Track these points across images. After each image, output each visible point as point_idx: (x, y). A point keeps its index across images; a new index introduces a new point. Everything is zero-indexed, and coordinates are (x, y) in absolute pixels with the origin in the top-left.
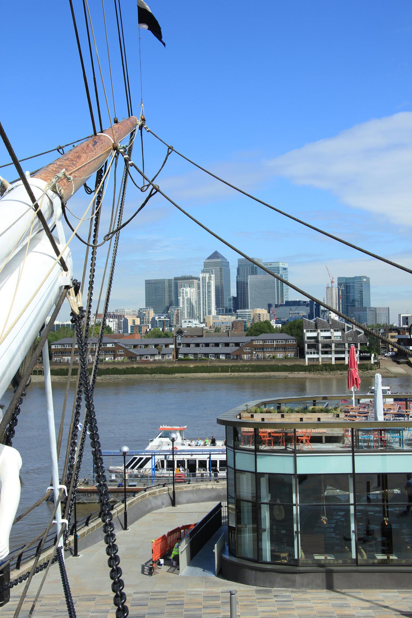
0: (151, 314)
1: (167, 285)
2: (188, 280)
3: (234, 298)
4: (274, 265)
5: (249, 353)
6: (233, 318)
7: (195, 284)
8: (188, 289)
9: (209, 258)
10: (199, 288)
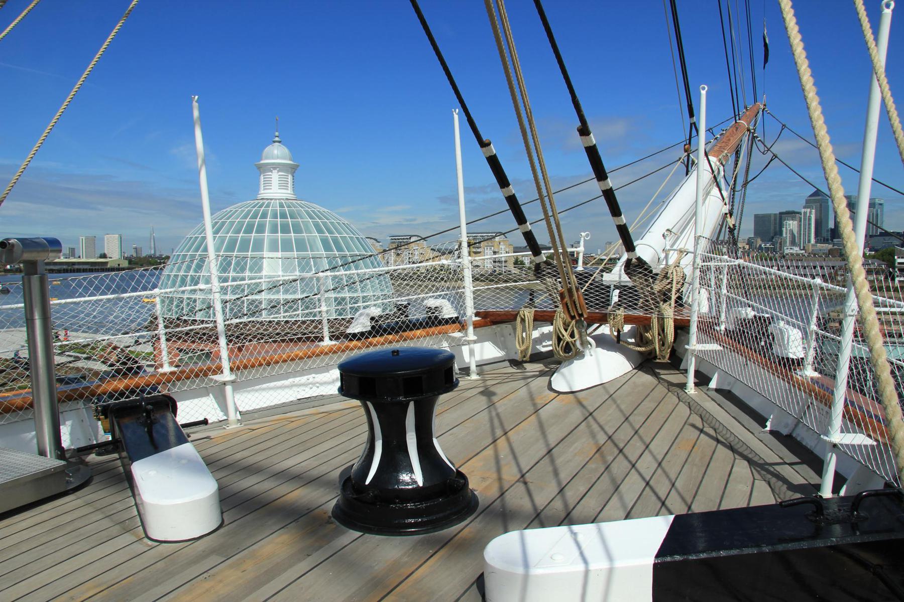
0: (759, 242)
1: (772, 218)
2: (792, 214)
3: (832, 230)
5: (842, 275)
6: (830, 246)
8: (791, 222)
9: (811, 196)
10: (800, 221)
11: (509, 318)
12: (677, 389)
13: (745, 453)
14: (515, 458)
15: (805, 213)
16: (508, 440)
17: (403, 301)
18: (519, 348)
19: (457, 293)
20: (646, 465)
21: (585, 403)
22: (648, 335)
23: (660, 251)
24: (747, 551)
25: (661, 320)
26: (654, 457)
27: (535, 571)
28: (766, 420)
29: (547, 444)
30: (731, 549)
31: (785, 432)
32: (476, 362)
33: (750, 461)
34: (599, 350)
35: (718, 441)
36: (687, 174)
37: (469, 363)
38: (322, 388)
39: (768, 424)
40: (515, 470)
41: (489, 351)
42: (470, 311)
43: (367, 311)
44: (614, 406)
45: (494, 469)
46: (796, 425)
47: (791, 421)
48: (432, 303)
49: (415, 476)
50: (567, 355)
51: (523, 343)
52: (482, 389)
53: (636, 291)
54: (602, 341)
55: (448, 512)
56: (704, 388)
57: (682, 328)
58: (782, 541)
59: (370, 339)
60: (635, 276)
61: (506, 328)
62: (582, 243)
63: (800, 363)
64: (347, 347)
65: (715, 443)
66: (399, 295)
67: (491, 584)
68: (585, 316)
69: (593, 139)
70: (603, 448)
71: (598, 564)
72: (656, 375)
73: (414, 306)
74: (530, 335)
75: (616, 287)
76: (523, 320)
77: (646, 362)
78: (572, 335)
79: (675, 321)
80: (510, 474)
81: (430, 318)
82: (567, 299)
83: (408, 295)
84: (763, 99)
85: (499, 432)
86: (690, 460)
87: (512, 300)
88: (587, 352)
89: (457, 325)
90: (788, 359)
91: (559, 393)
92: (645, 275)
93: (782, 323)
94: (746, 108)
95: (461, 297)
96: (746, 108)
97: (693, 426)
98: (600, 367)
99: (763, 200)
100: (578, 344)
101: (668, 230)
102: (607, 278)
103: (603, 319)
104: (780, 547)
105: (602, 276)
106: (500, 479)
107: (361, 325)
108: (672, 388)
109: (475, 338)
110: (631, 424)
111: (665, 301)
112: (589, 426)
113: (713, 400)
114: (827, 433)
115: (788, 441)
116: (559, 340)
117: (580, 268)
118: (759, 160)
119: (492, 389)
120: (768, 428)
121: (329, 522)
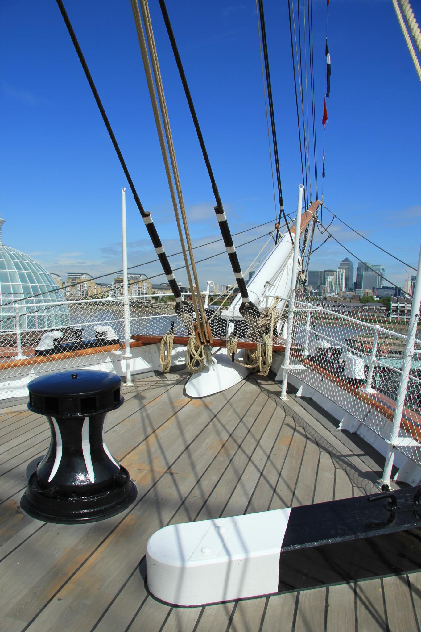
1: (320, 274)
2: (331, 272)
4: (377, 267)
6: (354, 293)
7: (335, 275)
8: (331, 277)
10: (336, 277)
11: (155, 341)
12: (274, 396)
13: (327, 447)
14: (163, 452)
15: (339, 272)
16: (156, 437)
19: (119, 322)
20: (259, 457)
21: (211, 407)
22: (253, 356)
23: (260, 296)
24: (347, 538)
25: (264, 346)
27: (189, 564)
28: (339, 422)
29: (185, 441)
30: (336, 537)
31: (352, 431)
32: (131, 372)
33: (330, 453)
34: (219, 365)
36: (276, 244)
37: (126, 373)
38: (15, 392)
39: (340, 425)
40: (163, 463)
41: (140, 364)
42: (128, 336)
43: (51, 334)
44: (232, 410)
46: (360, 426)
47: (356, 423)
48: (100, 328)
49: (88, 476)
50: (196, 368)
51: (165, 359)
52: (134, 394)
53: (247, 325)
54: (222, 360)
55: (113, 503)
57: (279, 351)
58: (369, 527)
59: (53, 355)
60: (247, 315)
61: (153, 347)
62: (208, 289)
63: (362, 383)
65: (305, 439)
66: (76, 323)
67: (151, 571)
68: (211, 342)
69: (225, 216)
70: (227, 444)
71: (238, 556)
72: (259, 385)
73: (87, 331)
74: (169, 353)
75: (231, 321)
76: (166, 343)
77: (251, 375)
78: (201, 355)
79: (274, 347)
80: (160, 466)
81: (98, 340)
82: (199, 330)
83: (83, 322)
84: (322, 198)
85: (149, 430)
86: (289, 453)
87: (158, 328)
88: (211, 368)
89: (118, 345)
90: (356, 380)
91: (192, 398)
92: (254, 314)
93: (350, 355)
94: (311, 202)
95: (121, 325)
97: (288, 425)
98: (219, 379)
99: (317, 264)
100: (205, 361)
101: (267, 282)
102: (226, 314)
103: (222, 344)
104: (371, 534)
105: (221, 312)
106: (152, 471)
107: (46, 344)
108: (271, 395)
110: (245, 425)
111: (267, 333)
112: (214, 426)
113: (300, 405)
114: (389, 438)
115: (354, 437)
116: (191, 358)
117: (206, 306)
119: (143, 394)
120: (340, 428)
121: (18, 513)
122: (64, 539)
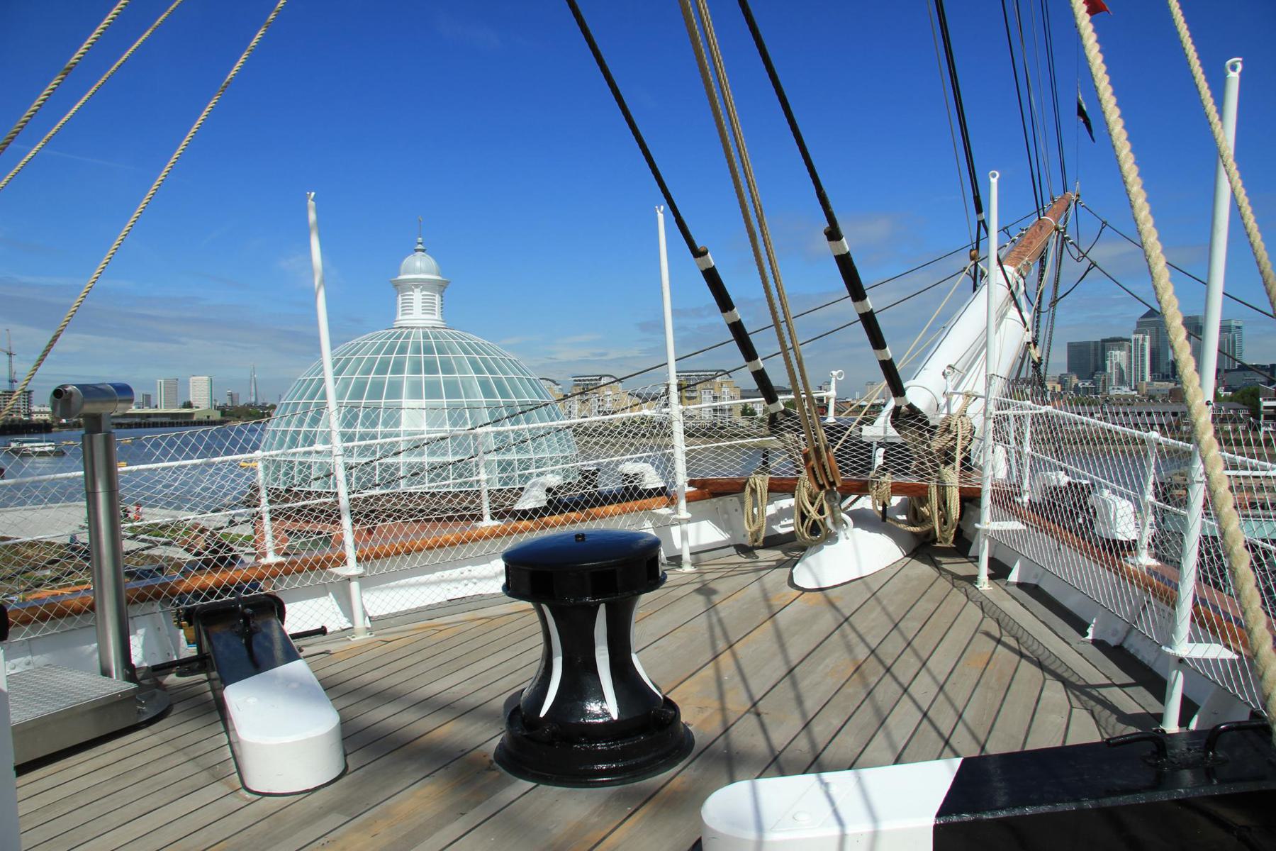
0: (1075, 380)
1: (1092, 347)
2: (1118, 342)
8: (1118, 353)
9: (1144, 317)
11: (733, 488)
12: (964, 584)
13: (1059, 671)
16: (734, 655)
17: (590, 465)
18: (748, 529)
19: (664, 455)
20: (923, 689)
21: (839, 604)
22: (924, 509)
23: (939, 395)
24: (1061, 807)
25: (942, 489)
26: (934, 678)
28: (1087, 626)
29: (787, 661)
31: (1113, 641)
33: (1067, 684)
34: (858, 530)
35: (1022, 655)
37: (681, 550)
38: (480, 584)
39: (1090, 631)
41: (708, 533)
42: (682, 479)
43: (542, 479)
44: (879, 609)
45: (715, 695)
47: (1121, 628)
48: (629, 468)
49: (607, 706)
52: (698, 586)
54: (861, 519)
55: (651, 755)
56: (1001, 582)
57: (970, 499)
59: (546, 518)
61: (731, 501)
62: (833, 385)
63: (1131, 546)
64: (515, 529)
65: (1017, 658)
66: (586, 458)
68: (838, 485)
69: (846, 245)
70: (864, 666)
71: (858, 827)
72: (936, 565)
74: (763, 512)
75: (880, 445)
76: (754, 491)
77: (922, 548)
78: (821, 511)
79: (961, 490)
80: (737, 702)
81: (627, 489)
82: (813, 462)
83: (598, 457)
85: (721, 645)
86: (982, 681)
87: (738, 463)
88: (841, 535)
90: (1114, 541)
91: (804, 590)
92: (920, 428)
93: (1106, 493)
94: (1052, 199)
95: (668, 460)
96: (1052, 199)
97: (988, 634)
98: (858, 555)
99: (1079, 323)
100: (829, 522)
102: (869, 432)
103: (862, 489)
105: (861, 430)
106: (723, 709)
107: (533, 499)
108: (957, 582)
109: (689, 515)
110: (902, 634)
111: (947, 463)
112: (844, 636)
114: (1170, 643)
115: (1118, 654)
116: (803, 517)
117: (831, 419)
118: (1072, 268)
119: (712, 585)
120: (1090, 637)
121: (490, 769)
122: (569, 808)
